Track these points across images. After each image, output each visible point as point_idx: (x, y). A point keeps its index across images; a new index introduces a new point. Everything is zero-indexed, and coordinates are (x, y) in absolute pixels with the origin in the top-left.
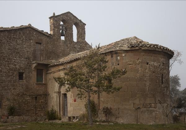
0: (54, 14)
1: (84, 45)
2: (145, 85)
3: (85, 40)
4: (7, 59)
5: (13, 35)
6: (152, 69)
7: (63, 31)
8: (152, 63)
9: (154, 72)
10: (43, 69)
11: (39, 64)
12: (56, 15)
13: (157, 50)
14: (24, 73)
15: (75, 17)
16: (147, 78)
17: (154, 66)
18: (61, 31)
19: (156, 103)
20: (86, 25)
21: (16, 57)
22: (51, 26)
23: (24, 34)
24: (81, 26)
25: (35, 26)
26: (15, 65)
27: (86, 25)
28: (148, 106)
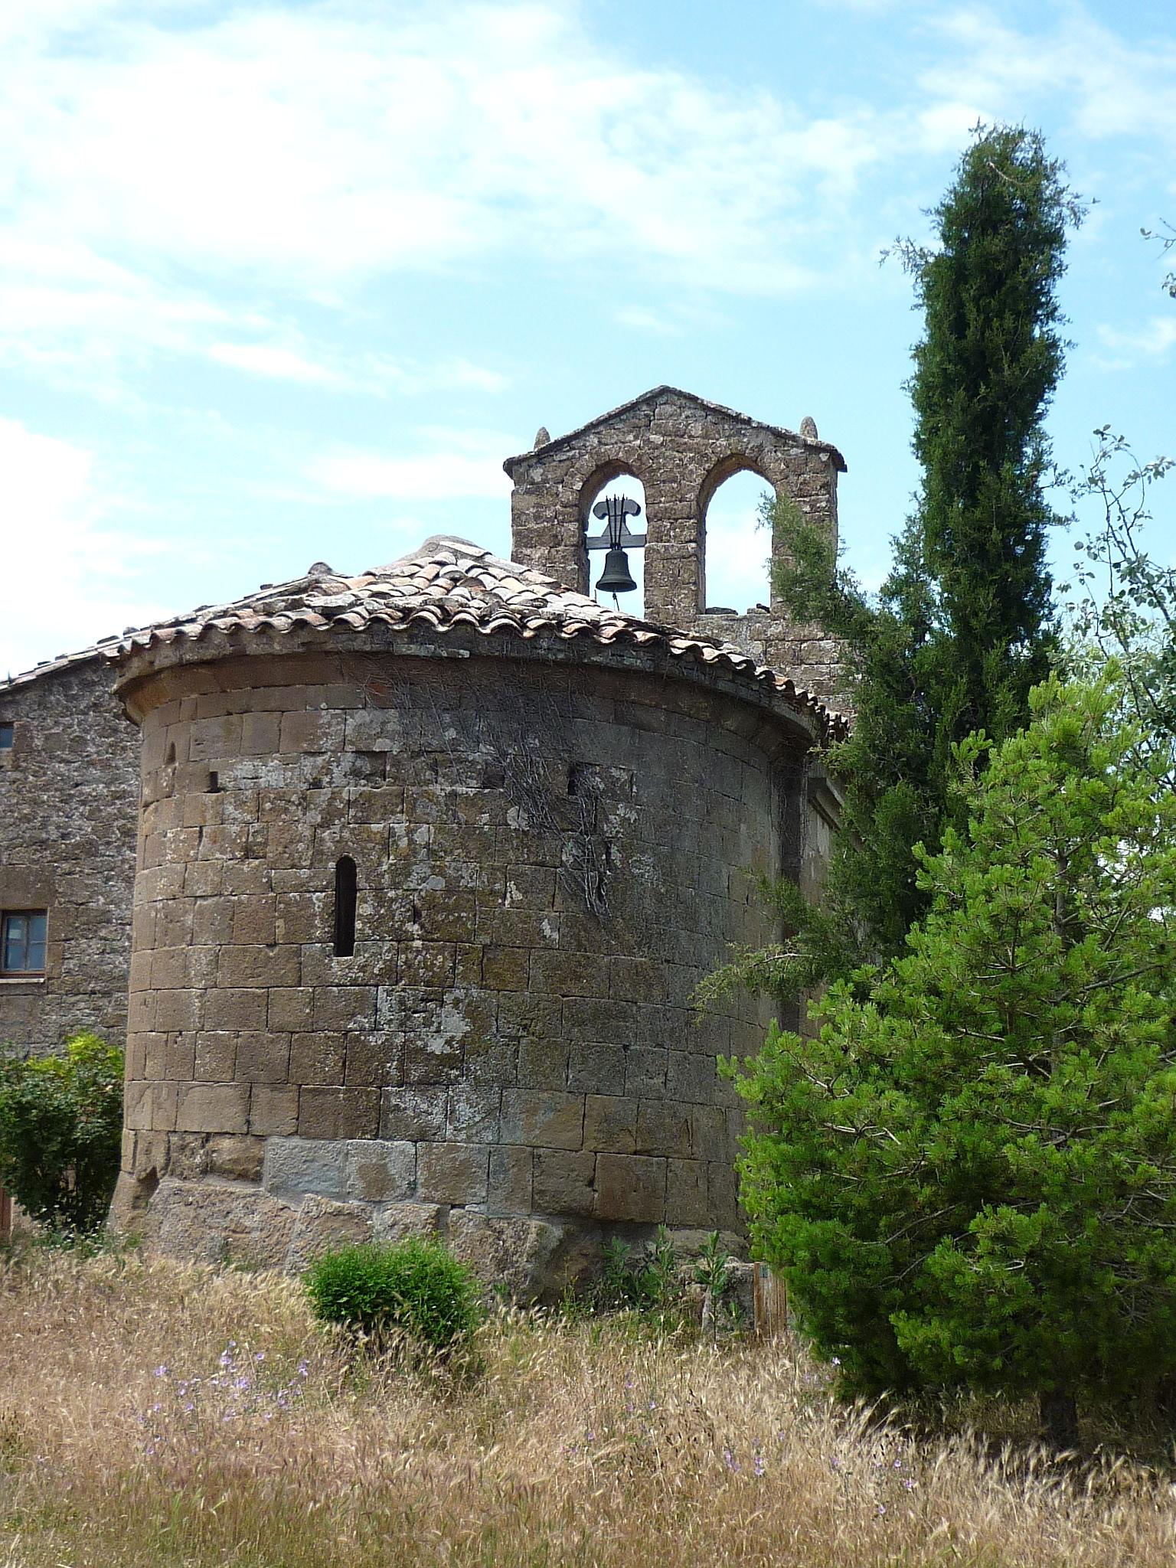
0: (544, 434)
6: (235, 828)
8: (245, 767)
9: (248, 853)
15: (721, 414)
16: (200, 913)
17: (260, 797)
19: (257, 1129)
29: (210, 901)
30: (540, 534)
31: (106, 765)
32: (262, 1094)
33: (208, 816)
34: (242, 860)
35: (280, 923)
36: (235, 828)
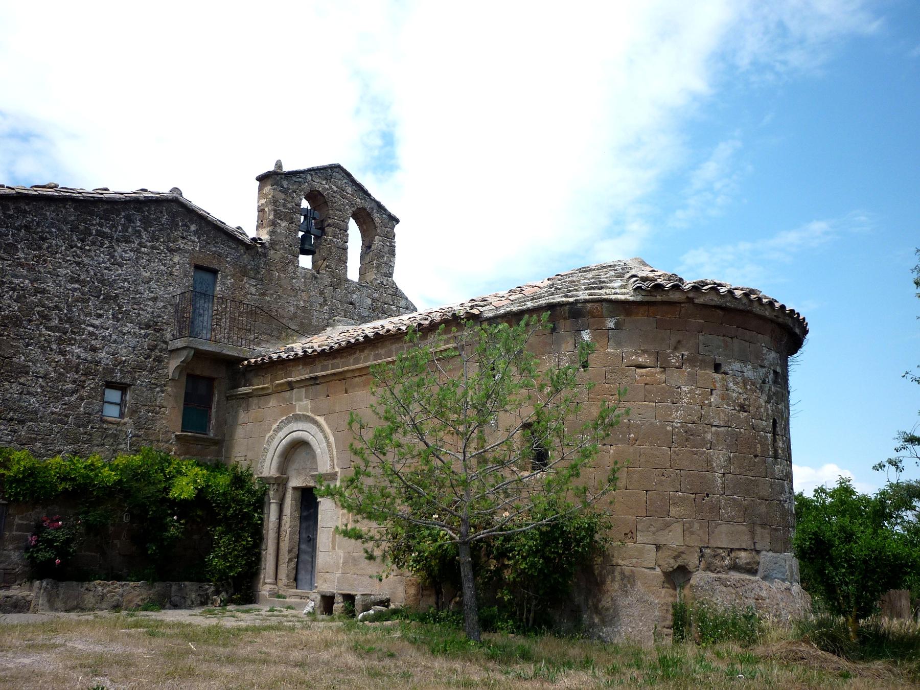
0: (279, 165)
1: (389, 299)
2: (709, 462)
3: (394, 278)
4: (61, 320)
5: (101, 225)
6: (735, 395)
7: (308, 233)
9: (743, 408)
10: (211, 380)
11: (199, 355)
12: (286, 169)
13: (757, 309)
14: (130, 385)
16: (717, 434)
18: (301, 234)
20: (397, 221)
21: (100, 316)
22: (261, 210)
23: (146, 223)
24: (377, 222)
25: (198, 197)
26: (94, 349)
27: (397, 221)
28: (723, 559)
29: (722, 429)
30: (286, 215)
31: (31, 269)
32: (759, 530)
33: (718, 385)
34: (739, 411)
35: (758, 446)
36: (735, 395)
